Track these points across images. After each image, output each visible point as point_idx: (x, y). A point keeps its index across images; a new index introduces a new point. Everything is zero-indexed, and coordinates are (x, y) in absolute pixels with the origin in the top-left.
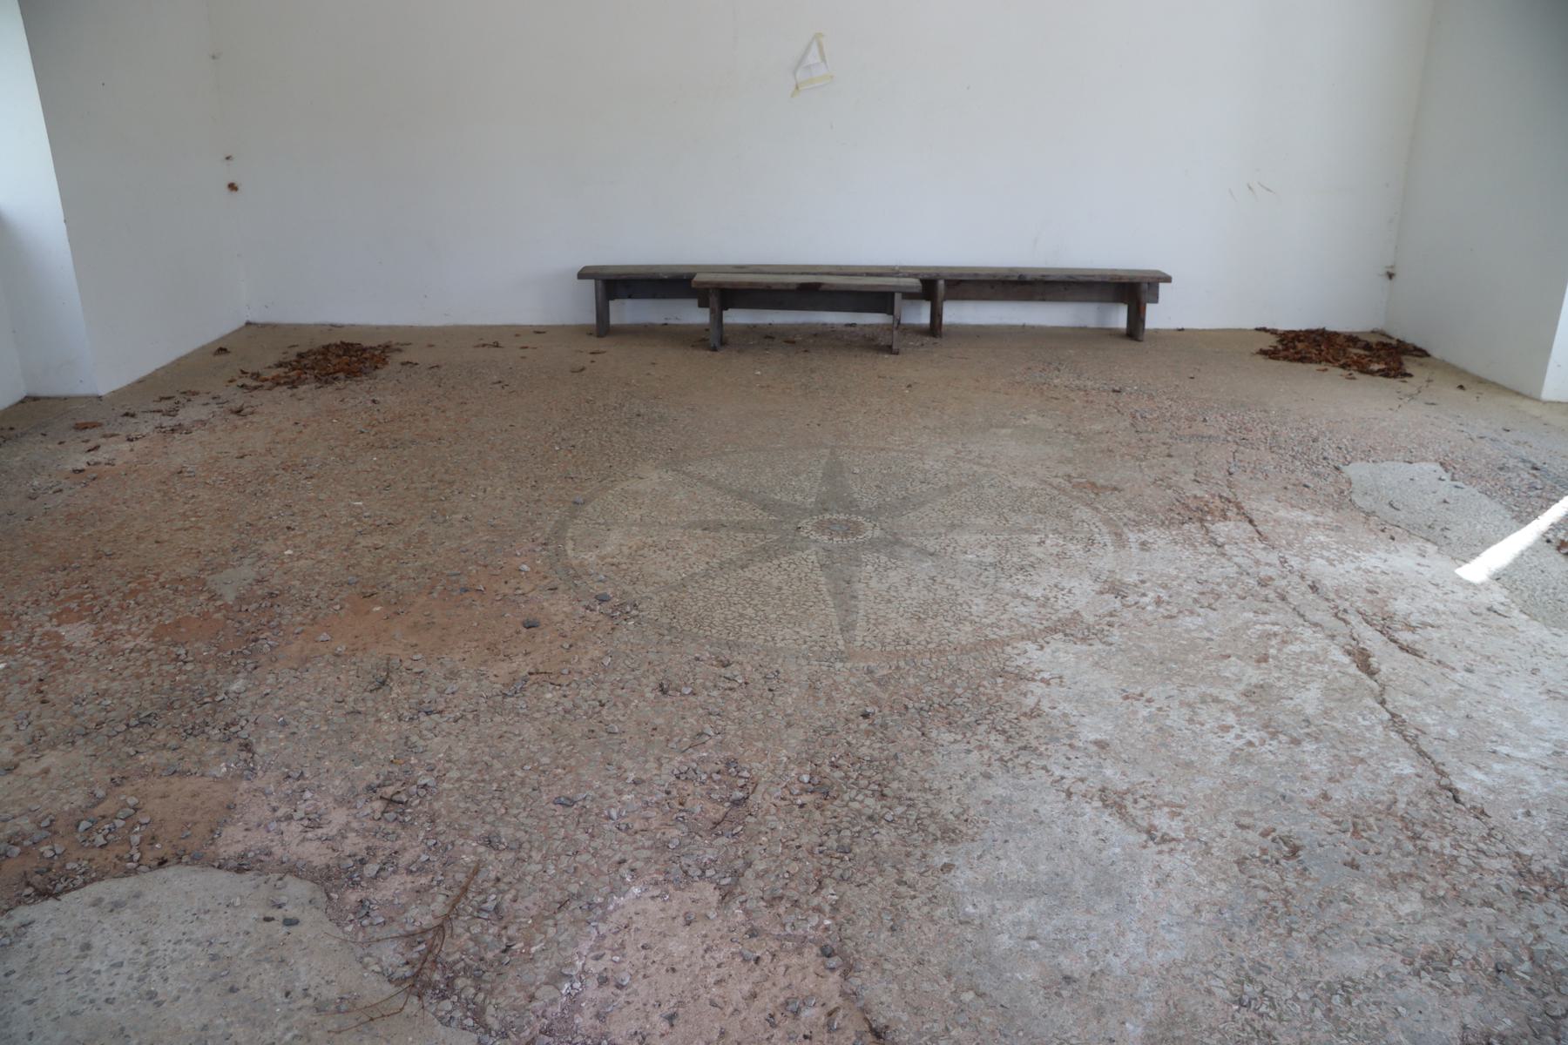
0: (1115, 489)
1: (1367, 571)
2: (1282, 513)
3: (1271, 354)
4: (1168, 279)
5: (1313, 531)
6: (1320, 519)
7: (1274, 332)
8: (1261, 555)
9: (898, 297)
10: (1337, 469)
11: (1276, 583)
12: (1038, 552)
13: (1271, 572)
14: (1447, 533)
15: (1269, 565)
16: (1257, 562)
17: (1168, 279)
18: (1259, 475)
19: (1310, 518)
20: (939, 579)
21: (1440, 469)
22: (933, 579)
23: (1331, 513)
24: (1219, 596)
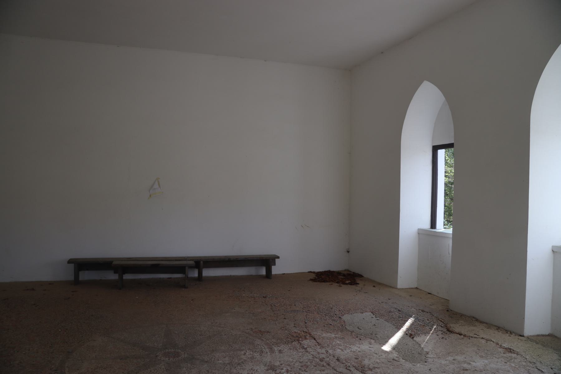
0: (268, 332)
1: (354, 352)
2: (324, 335)
3: (313, 280)
4: (278, 257)
5: (335, 340)
6: (337, 336)
7: (314, 272)
8: (319, 350)
9: (187, 268)
10: (340, 318)
11: (326, 360)
12: (243, 357)
13: (323, 356)
14: (377, 336)
15: (323, 353)
16: (318, 353)
17: (278, 257)
18: (315, 323)
19: (333, 336)
20: (210, 371)
21: (371, 314)
22: (208, 371)
23: (340, 333)
24: (307, 367)
